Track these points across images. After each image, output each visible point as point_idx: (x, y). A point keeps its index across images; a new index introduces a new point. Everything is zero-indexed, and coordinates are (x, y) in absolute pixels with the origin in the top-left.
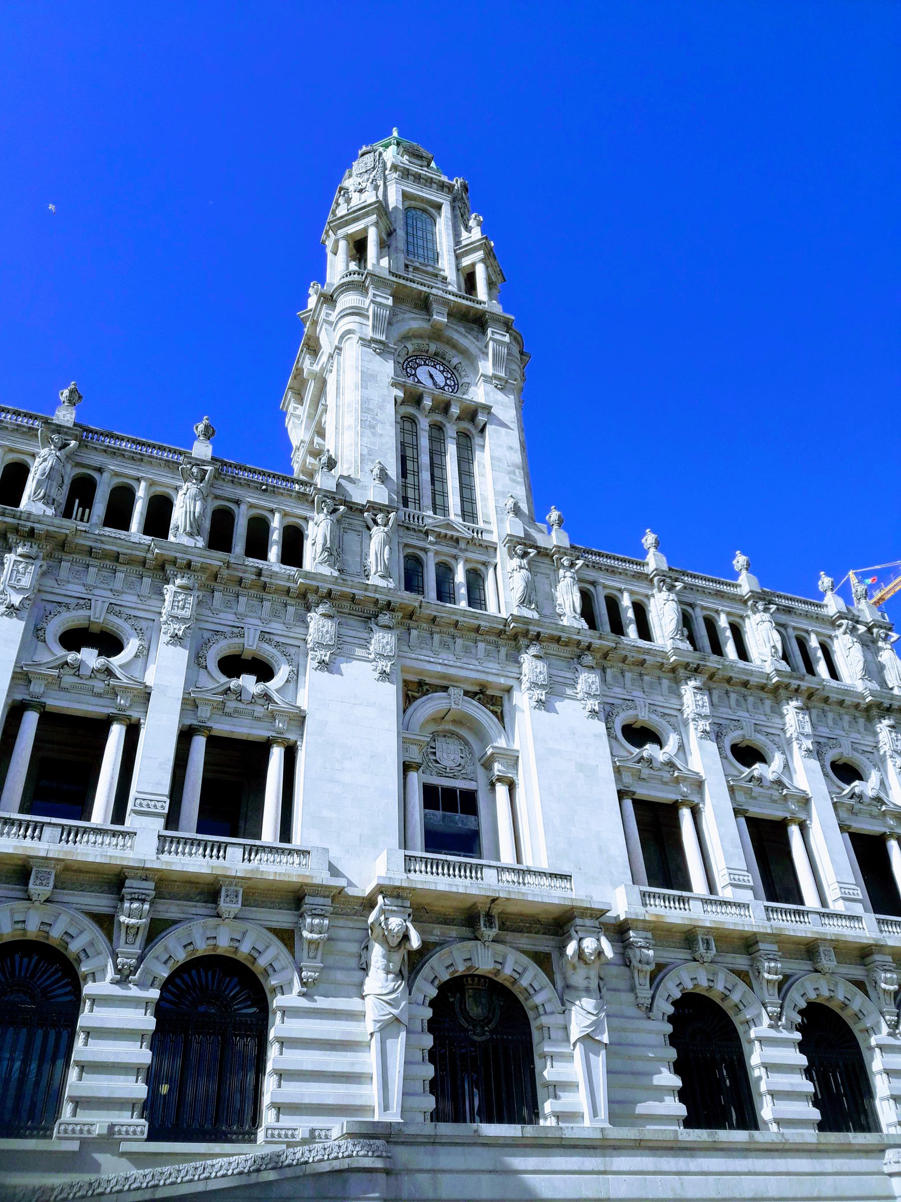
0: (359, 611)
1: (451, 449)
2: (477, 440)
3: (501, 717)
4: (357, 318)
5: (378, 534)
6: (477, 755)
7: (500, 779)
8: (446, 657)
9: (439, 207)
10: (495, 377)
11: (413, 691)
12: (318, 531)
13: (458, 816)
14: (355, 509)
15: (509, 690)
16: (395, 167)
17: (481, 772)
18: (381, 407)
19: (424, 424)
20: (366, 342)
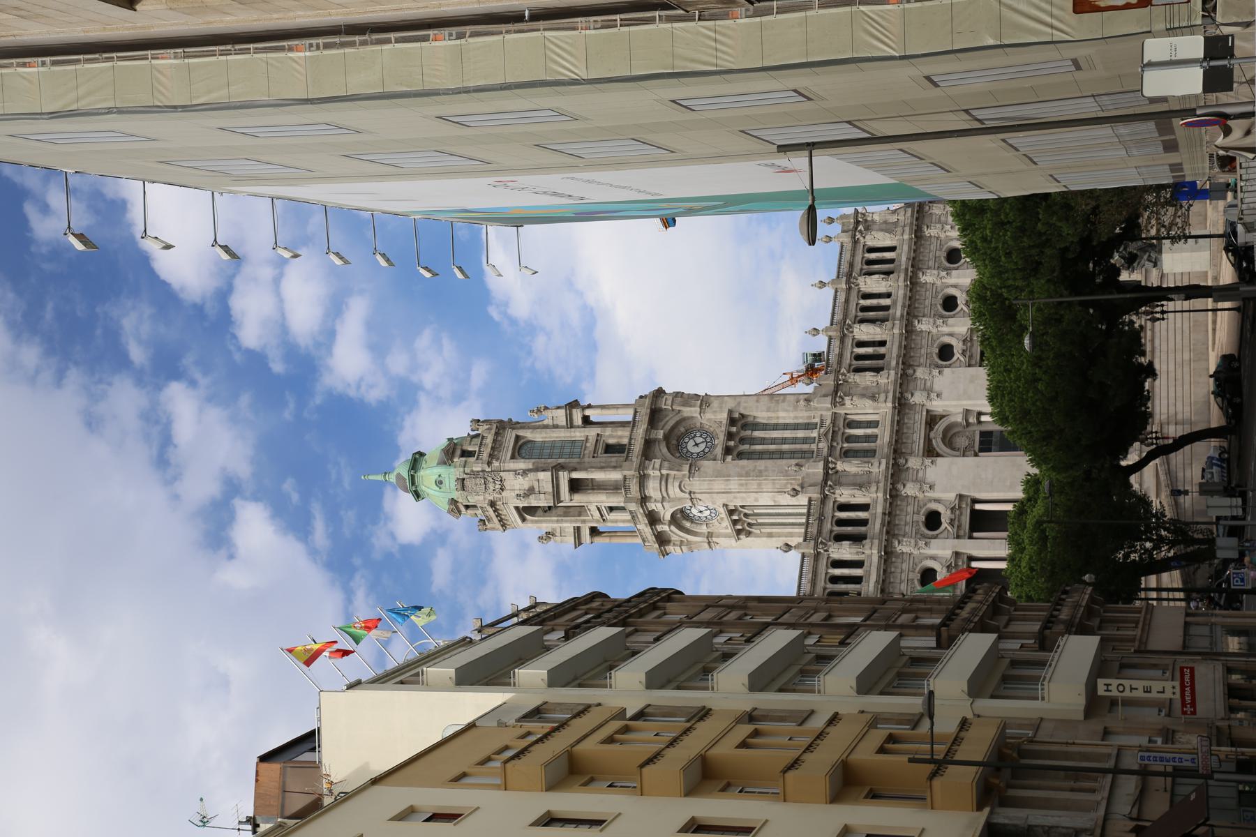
0: (897, 473)
1: (757, 434)
2: (751, 419)
3: (942, 417)
4: (670, 480)
5: (840, 466)
6: (960, 429)
7: (978, 419)
8: (916, 437)
9: (518, 437)
10: (701, 406)
11: (930, 452)
12: (845, 495)
13: (994, 439)
14: (826, 476)
15: (928, 411)
16: (489, 463)
17: (971, 428)
18: (743, 467)
19: (745, 447)
20: (691, 474)
